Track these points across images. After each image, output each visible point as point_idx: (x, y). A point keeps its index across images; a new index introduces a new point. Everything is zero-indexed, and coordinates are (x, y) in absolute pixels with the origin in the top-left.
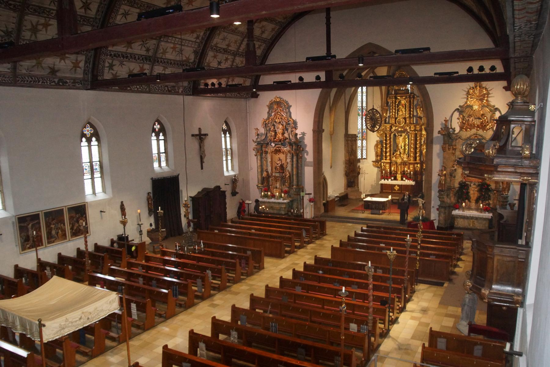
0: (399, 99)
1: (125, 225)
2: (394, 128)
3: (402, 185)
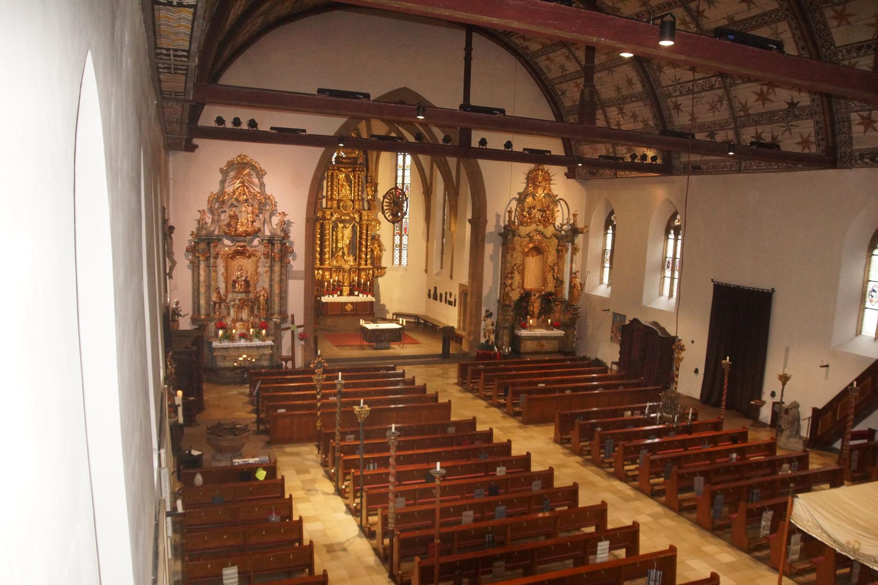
0: (342, 171)
1: (784, 384)
2: (335, 216)
3: (356, 303)
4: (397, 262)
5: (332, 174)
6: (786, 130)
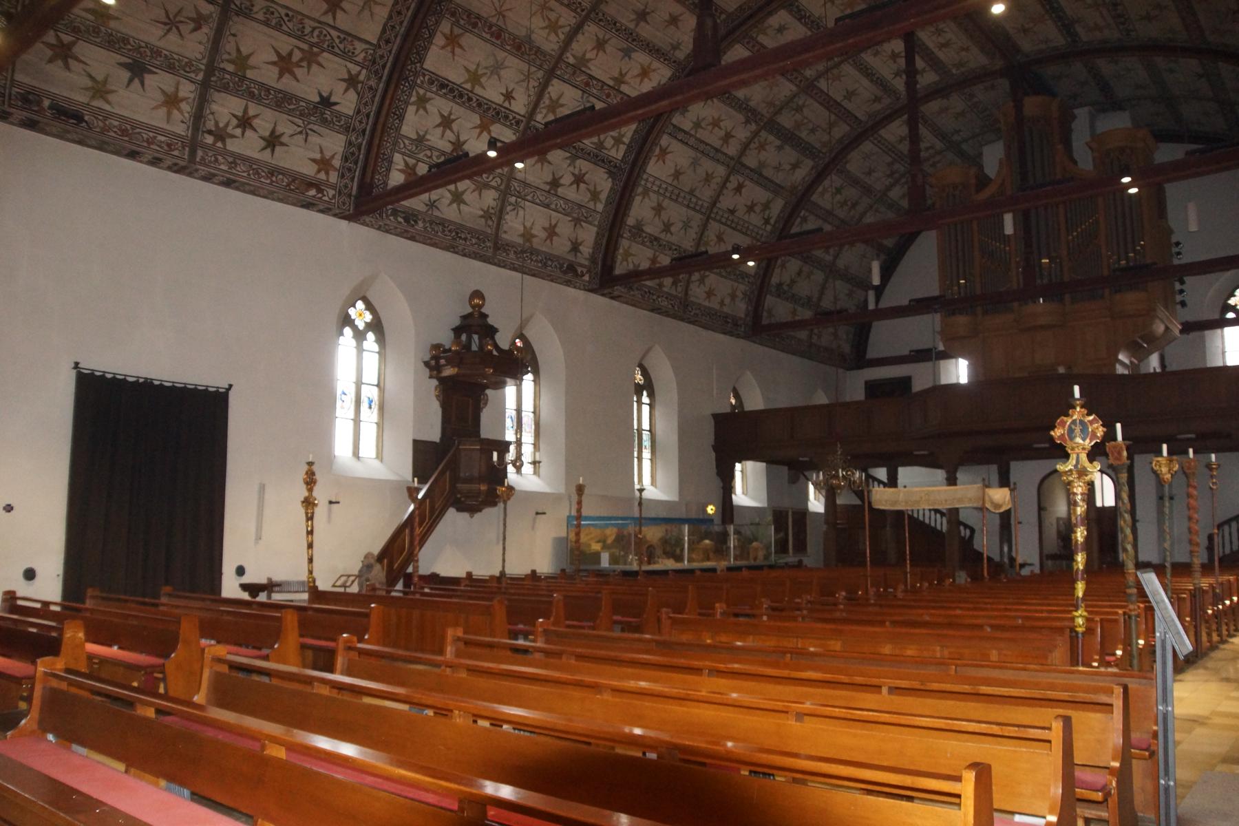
6: (301, 133)
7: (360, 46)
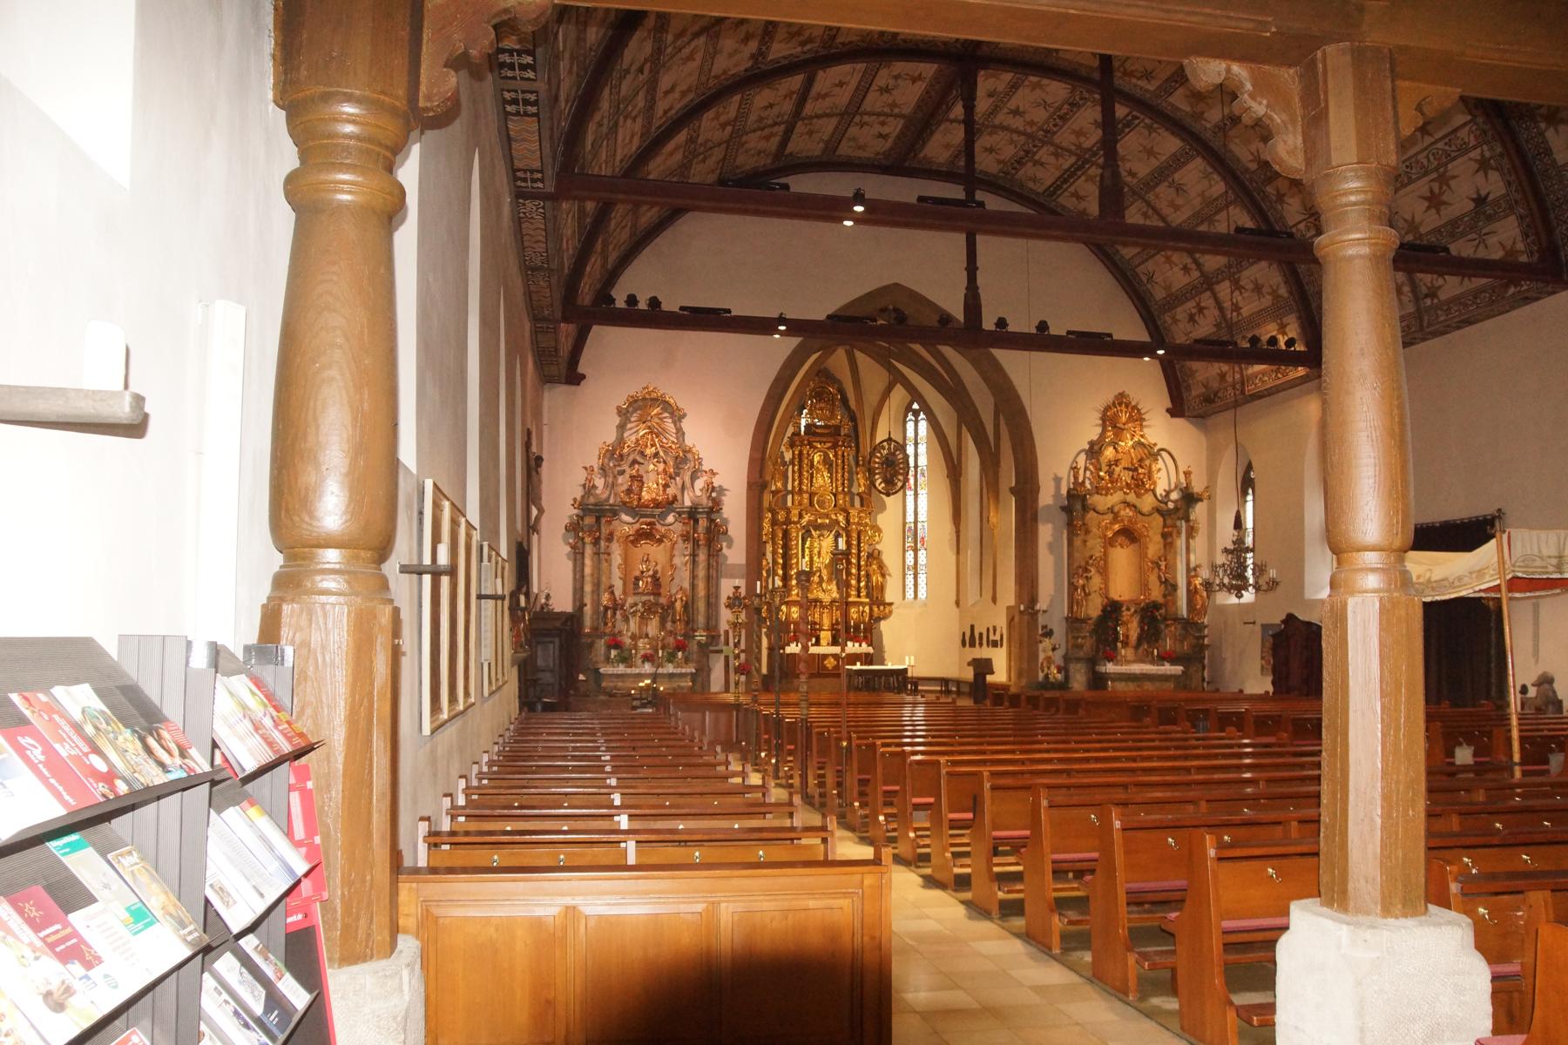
0: (816, 448)
2: (807, 518)
4: (910, 594)
5: (801, 453)
7: (1463, 133)
